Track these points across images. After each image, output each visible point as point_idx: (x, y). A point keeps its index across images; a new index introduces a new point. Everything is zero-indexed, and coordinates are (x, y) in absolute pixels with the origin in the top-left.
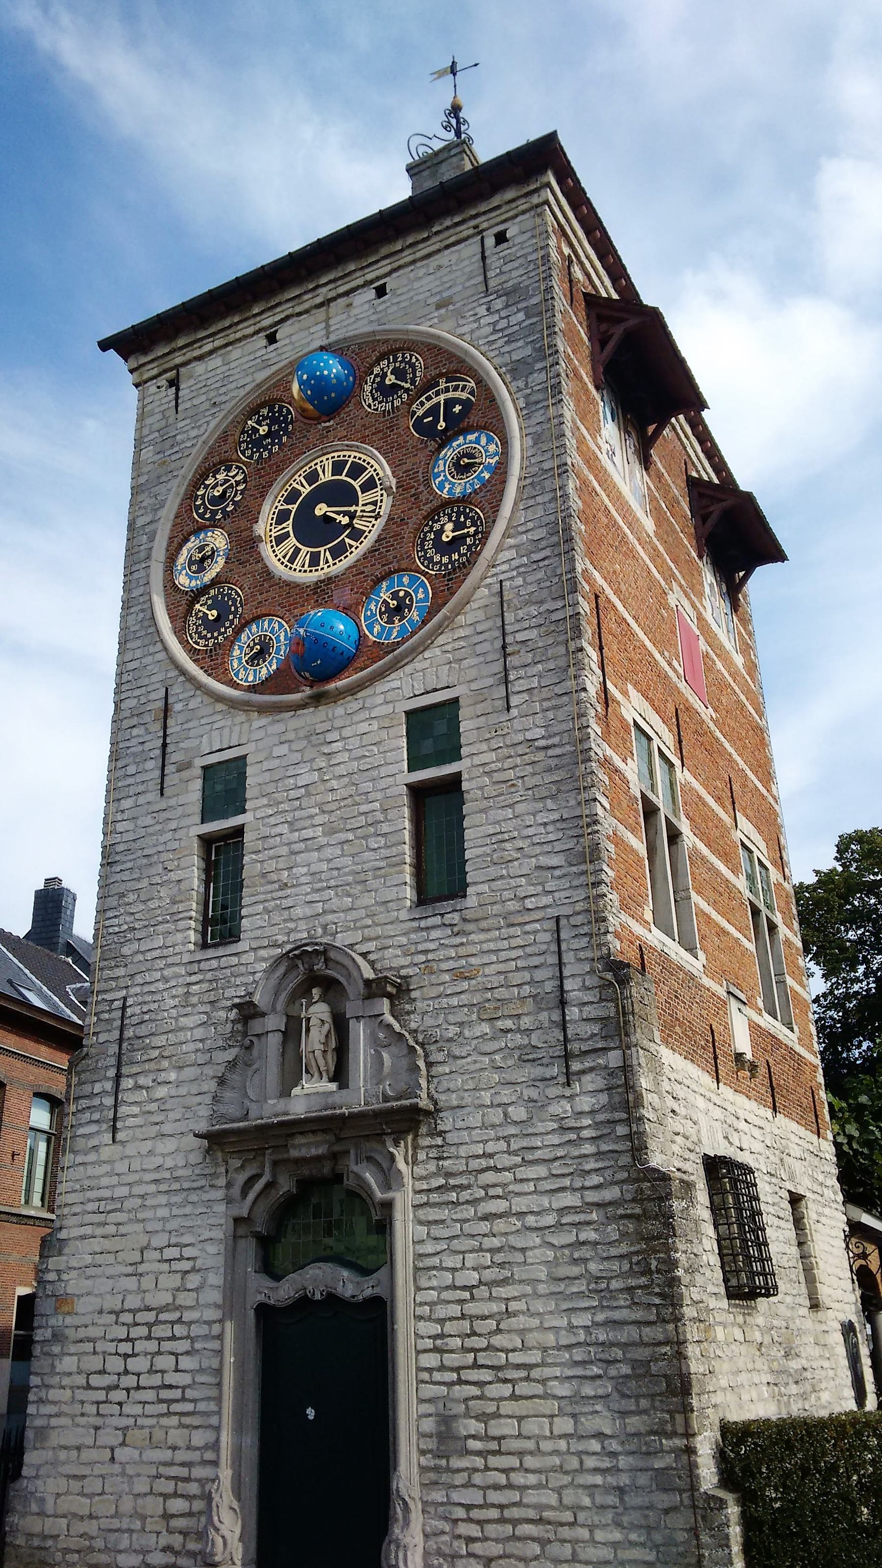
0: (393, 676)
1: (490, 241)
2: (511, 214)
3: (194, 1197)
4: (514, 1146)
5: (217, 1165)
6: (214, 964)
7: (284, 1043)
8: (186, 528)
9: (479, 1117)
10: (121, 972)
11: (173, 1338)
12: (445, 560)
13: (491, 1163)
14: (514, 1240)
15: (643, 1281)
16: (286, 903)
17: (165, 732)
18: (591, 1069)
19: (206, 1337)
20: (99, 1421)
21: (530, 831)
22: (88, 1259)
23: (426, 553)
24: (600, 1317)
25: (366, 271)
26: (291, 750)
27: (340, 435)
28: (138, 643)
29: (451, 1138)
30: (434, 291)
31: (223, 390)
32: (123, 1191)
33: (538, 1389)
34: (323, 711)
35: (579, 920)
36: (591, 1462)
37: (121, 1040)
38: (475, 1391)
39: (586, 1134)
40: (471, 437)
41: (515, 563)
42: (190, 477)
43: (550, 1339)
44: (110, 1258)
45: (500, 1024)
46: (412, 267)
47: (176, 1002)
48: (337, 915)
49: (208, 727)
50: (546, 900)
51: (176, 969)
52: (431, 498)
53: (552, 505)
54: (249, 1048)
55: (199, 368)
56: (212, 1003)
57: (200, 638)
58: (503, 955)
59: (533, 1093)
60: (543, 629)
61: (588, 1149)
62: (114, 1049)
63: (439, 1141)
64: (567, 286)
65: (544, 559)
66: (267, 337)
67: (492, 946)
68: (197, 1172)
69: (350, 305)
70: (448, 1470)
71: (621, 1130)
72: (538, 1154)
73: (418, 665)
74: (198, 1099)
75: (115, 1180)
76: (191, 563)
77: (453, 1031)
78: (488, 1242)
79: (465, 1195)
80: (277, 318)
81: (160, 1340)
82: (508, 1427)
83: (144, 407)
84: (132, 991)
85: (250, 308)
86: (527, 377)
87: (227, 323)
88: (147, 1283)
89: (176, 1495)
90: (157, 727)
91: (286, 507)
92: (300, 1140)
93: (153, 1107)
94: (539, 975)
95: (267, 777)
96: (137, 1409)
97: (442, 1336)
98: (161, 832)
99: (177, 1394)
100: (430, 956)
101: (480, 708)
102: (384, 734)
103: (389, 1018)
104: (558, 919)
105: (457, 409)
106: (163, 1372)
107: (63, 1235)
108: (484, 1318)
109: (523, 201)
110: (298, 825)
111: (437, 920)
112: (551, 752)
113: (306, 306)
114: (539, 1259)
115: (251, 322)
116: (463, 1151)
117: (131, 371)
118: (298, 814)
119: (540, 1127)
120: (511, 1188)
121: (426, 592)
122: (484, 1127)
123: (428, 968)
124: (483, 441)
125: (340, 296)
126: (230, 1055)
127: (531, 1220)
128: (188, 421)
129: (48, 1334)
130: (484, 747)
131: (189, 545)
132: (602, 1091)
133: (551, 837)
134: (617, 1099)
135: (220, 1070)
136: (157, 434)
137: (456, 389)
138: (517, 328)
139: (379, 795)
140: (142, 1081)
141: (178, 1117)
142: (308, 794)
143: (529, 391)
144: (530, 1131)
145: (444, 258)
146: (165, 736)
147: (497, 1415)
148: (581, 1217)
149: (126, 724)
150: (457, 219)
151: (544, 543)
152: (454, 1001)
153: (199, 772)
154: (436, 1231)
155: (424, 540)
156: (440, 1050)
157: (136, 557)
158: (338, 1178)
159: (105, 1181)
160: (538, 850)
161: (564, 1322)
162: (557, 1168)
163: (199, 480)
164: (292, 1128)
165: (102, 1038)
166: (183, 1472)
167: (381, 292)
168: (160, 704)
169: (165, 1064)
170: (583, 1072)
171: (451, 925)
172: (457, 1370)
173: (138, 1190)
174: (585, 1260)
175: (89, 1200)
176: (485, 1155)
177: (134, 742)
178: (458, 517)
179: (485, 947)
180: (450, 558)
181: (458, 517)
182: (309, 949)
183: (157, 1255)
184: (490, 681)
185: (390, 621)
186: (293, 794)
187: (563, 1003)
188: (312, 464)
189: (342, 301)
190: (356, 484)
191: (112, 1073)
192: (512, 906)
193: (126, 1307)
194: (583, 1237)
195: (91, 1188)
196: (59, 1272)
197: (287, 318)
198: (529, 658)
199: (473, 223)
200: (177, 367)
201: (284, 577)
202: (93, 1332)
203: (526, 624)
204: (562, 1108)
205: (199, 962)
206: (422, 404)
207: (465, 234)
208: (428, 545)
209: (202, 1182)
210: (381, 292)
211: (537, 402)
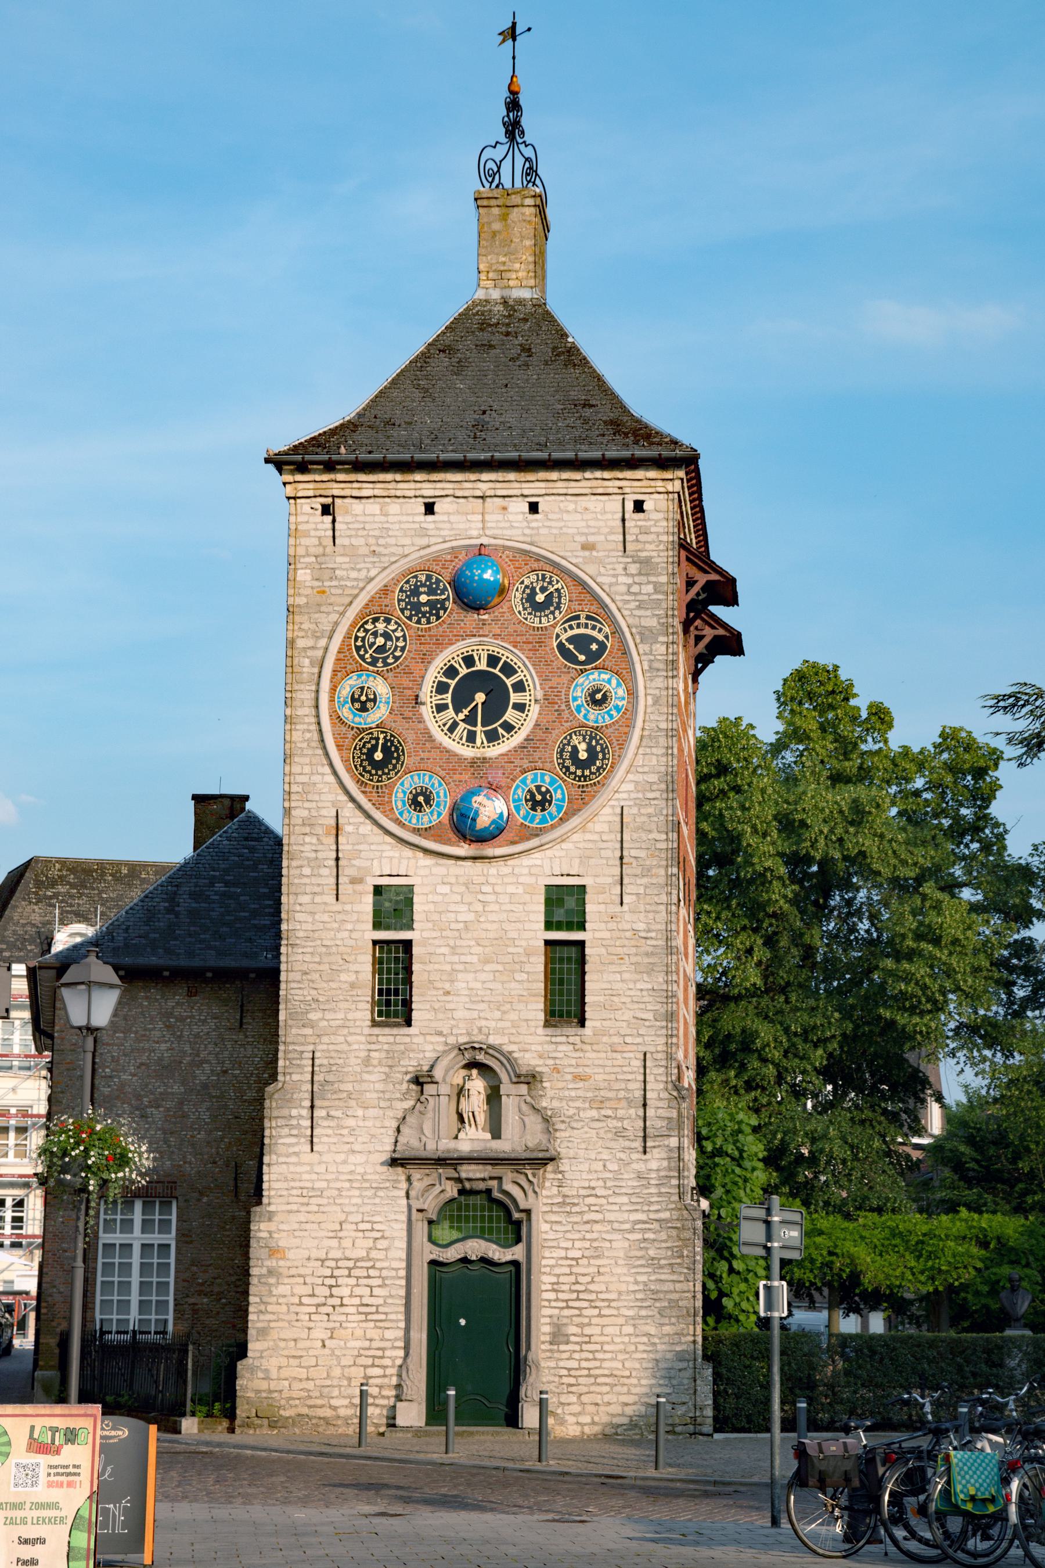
0: (537, 855)
1: (630, 506)
10: (308, 1031)
11: (369, 1277)
12: (579, 773)
14: (604, 1236)
15: (679, 1261)
16: (449, 1006)
19: (393, 1278)
20: (312, 1325)
22: (296, 1226)
24: (653, 1278)
28: (307, 760)
29: (567, 1175)
31: (381, 541)
32: (324, 1185)
33: (615, 1312)
34: (479, 866)
35: (659, 1056)
36: (641, 1347)
38: (577, 1312)
39: (653, 1182)
40: (605, 676)
41: (633, 795)
43: (623, 1287)
44: (315, 1226)
45: (603, 1112)
46: (562, 498)
49: (378, 854)
50: (639, 1040)
51: (359, 1038)
55: (357, 506)
56: (390, 1067)
58: (608, 1070)
59: (622, 1156)
61: (653, 1190)
63: (560, 1176)
67: (601, 1062)
70: (559, 1351)
71: (675, 1182)
72: (624, 1190)
73: (556, 851)
74: (383, 1130)
75: (314, 1177)
77: (571, 1112)
78: (588, 1236)
79: (575, 1209)
81: (358, 1278)
82: (597, 1330)
84: (320, 1047)
88: (347, 1243)
89: (373, 1365)
91: (444, 680)
92: (465, 1167)
93: (345, 1132)
94: (631, 1086)
95: (431, 907)
96: (343, 1318)
97: (558, 1283)
98: (339, 930)
99: (374, 1309)
101: (601, 898)
102: (527, 897)
103: (529, 1099)
106: (361, 1297)
107: (272, 1208)
108: (584, 1275)
109: (660, 483)
110: (459, 951)
111: (563, 1039)
112: (649, 942)
114: (620, 1244)
115: (412, 485)
116: (576, 1184)
118: (459, 942)
119: (625, 1176)
121: (563, 794)
122: (590, 1171)
123: (556, 1070)
124: (614, 682)
127: (616, 1226)
128: (347, 559)
129: (264, 1271)
130: (603, 926)
131: (351, 682)
133: (646, 999)
134: (673, 1164)
135: (400, 1115)
136: (313, 559)
137: (594, 628)
139: (524, 943)
140: (332, 1113)
145: (592, 502)
146: (337, 850)
147: (589, 1324)
148: (647, 1226)
151: (655, 787)
152: (573, 1094)
153: (372, 889)
154: (555, 1227)
155: (563, 750)
156: (563, 1122)
159: (305, 1177)
160: (636, 1006)
161: (632, 1279)
165: (295, 1077)
166: (380, 1353)
167: (534, 508)
168: (333, 822)
169: (353, 1103)
172: (567, 1301)
174: (647, 1249)
177: (307, 848)
179: (596, 1062)
182: (477, 1046)
183: (354, 1227)
184: (610, 880)
185: (533, 809)
186: (453, 926)
187: (645, 1105)
190: (509, 682)
191: (308, 1104)
192: (616, 1039)
193: (330, 1256)
194: (646, 1236)
195: (293, 1180)
196: (270, 1232)
198: (639, 871)
200: (333, 497)
201: (445, 744)
202: (302, 1271)
203: (637, 845)
204: (640, 1167)
207: (610, 491)
208: (566, 755)
209: (388, 1184)
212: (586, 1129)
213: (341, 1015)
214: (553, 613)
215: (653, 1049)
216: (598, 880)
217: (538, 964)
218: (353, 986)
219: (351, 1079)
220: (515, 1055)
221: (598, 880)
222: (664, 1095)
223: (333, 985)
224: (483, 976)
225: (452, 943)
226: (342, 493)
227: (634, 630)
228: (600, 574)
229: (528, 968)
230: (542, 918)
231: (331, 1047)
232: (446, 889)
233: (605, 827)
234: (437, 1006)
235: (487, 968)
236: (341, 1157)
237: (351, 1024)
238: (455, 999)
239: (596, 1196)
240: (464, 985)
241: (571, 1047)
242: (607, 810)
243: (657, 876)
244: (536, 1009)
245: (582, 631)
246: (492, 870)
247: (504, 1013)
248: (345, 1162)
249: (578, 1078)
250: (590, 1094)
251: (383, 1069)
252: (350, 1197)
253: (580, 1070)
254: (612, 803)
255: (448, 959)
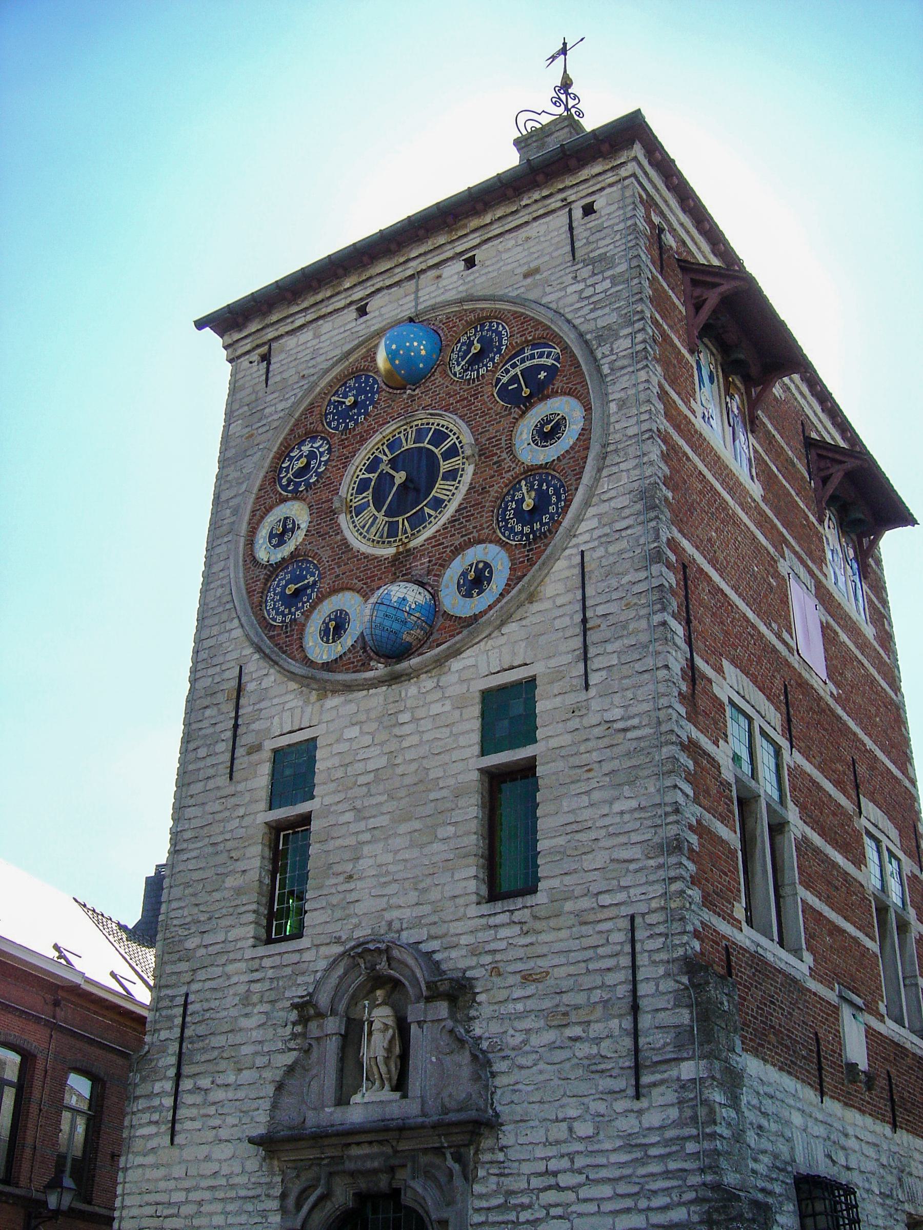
1: (578, 213)
2: (598, 187)
3: (249, 1207)
4: (580, 1162)
5: (273, 1174)
6: (277, 960)
7: (343, 1049)
8: (269, 501)
9: (542, 1132)
10: (183, 966)
12: (527, 530)
13: (552, 1181)
17: (237, 712)
18: (662, 1082)
21: (607, 821)
23: (507, 523)
25: (457, 244)
26: (361, 732)
27: (424, 404)
28: (216, 620)
29: (513, 1154)
30: (522, 262)
32: (179, 1197)
37: (182, 1039)
39: (653, 1152)
41: (596, 534)
42: (275, 449)
45: (569, 1032)
47: (236, 1001)
48: (401, 910)
50: (621, 897)
52: (514, 466)
53: (637, 472)
54: (308, 1051)
55: (290, 342)
57: (277, 614)
58: (573, 957)
59: (601, 1107)
60: (624, 602)
62: (174, 1047)
63: (500, 1156)
64: (656, 253)
65: (626, 528)
66: (357, 309)
68: (253, 1180)
69: (439, 277)
72: (603, 1173)
75: (172, 1184)
76: (271, 536)
77: (519, 1038)
79: (524, 1216)
80: (369, 291)
83: (235, 382)
84: (195, 987)
85: (340, 284)
86: (612, 344)
87: (319, 297)
90: (231, 706)
91: (367, 476)
93: (212, 1110)
94: (611, 979)
95: (336, 761)
100: (498, 957)
102: (457, 713)
103: (450, 1024)
104: (633, 918)
105: (543, 375)
111: (504, 918)
112: (630, 735)
113: (396, 279)
115: (343, 296)
116: (526, 1168)
117: (226, 347)
119: (608, 1146)
120: (573, 1208)
122: (547, 1143)
123: (496, 971)
125: (430, 268)
126: (289, 1058)
132: (672, 1105)
134: (688, 1113)
135: (278, 1075)
136: (246, 408)
137: (541, 356)
138: (603, 295)
139: (451, 782)
141: (236, 1121)
142: (377, 780)
143: (614, 357)
144: (596, 1147)
146: (237, 718)
149: (200, 703)
150: (545, 193)
151: (627, 512)
152: (520, 1007)
155: (506, 509)
156: (504, 1058)
157: (218, 532)
158: (396, 1193)
159: (162, 1185)
162: (622, 1188)
163: (284, 453)
164: (350, 1135)
165: (164, 1035)
167: (470, 263)
168: (234, 683)
169: (223, 1065)
170: (654, 1085)
171: (520, 923)
173: (195, 1196)
175: (147, 1204)
176: (547, 1172)
177: (205, 724)
178: (540, 485)
180: (532, 528)
181: (540, 485)
182: (371, 946)
186: (362, 780)
187: (635, 1009)
188: (396, 433)
189: (432, 274)
191: (172, 1072)
192: (585, 903)
197: (379, 290)
198: (608, 634)
199: (561, 196)
204: (628, 1124)
205: (262, 958)
206: (507, 371)
207: (553, 207)
208: (510, 514)
210: (470, 263)
211: (623, 368)
212: (542, 1066)
213: (221, 937)
214: (492, 359)
215: (643, 908)
216: (553, 663)
217: (471, 810)
218: (239, 891)
219: (226, 1028)
220: (437, 957)
221: (553, 663)
222: (668, 985)
223: (217, 896)
224: (398, 843)
225: (358, 804)
226: (276, 334)
227: (588, 337)
228: (545, 294)
229: (457, 816)
230: (476, 737)
231: (208, 985)
232: (354, 732)
233: (560, 587)
234: (334, 900)
235: (403, 828)
236: (203, 1151)
237: (231, 947)
238: (360, 885)
239: (558, 1188)
240: (371, 862)
241: (516, 929)
242: (561, 564)
243: (636, 632)
244: (467, 878)
245: (528, 364)
246: (411, 690)
247: (425, 890)
248: (208, 1158)
249: (527, 978)
250: (547, 1004)
251: (266, 1007)
252: (211, 1214)
253: (531, 964)
254: (567, 552)
255: (353, 828)
